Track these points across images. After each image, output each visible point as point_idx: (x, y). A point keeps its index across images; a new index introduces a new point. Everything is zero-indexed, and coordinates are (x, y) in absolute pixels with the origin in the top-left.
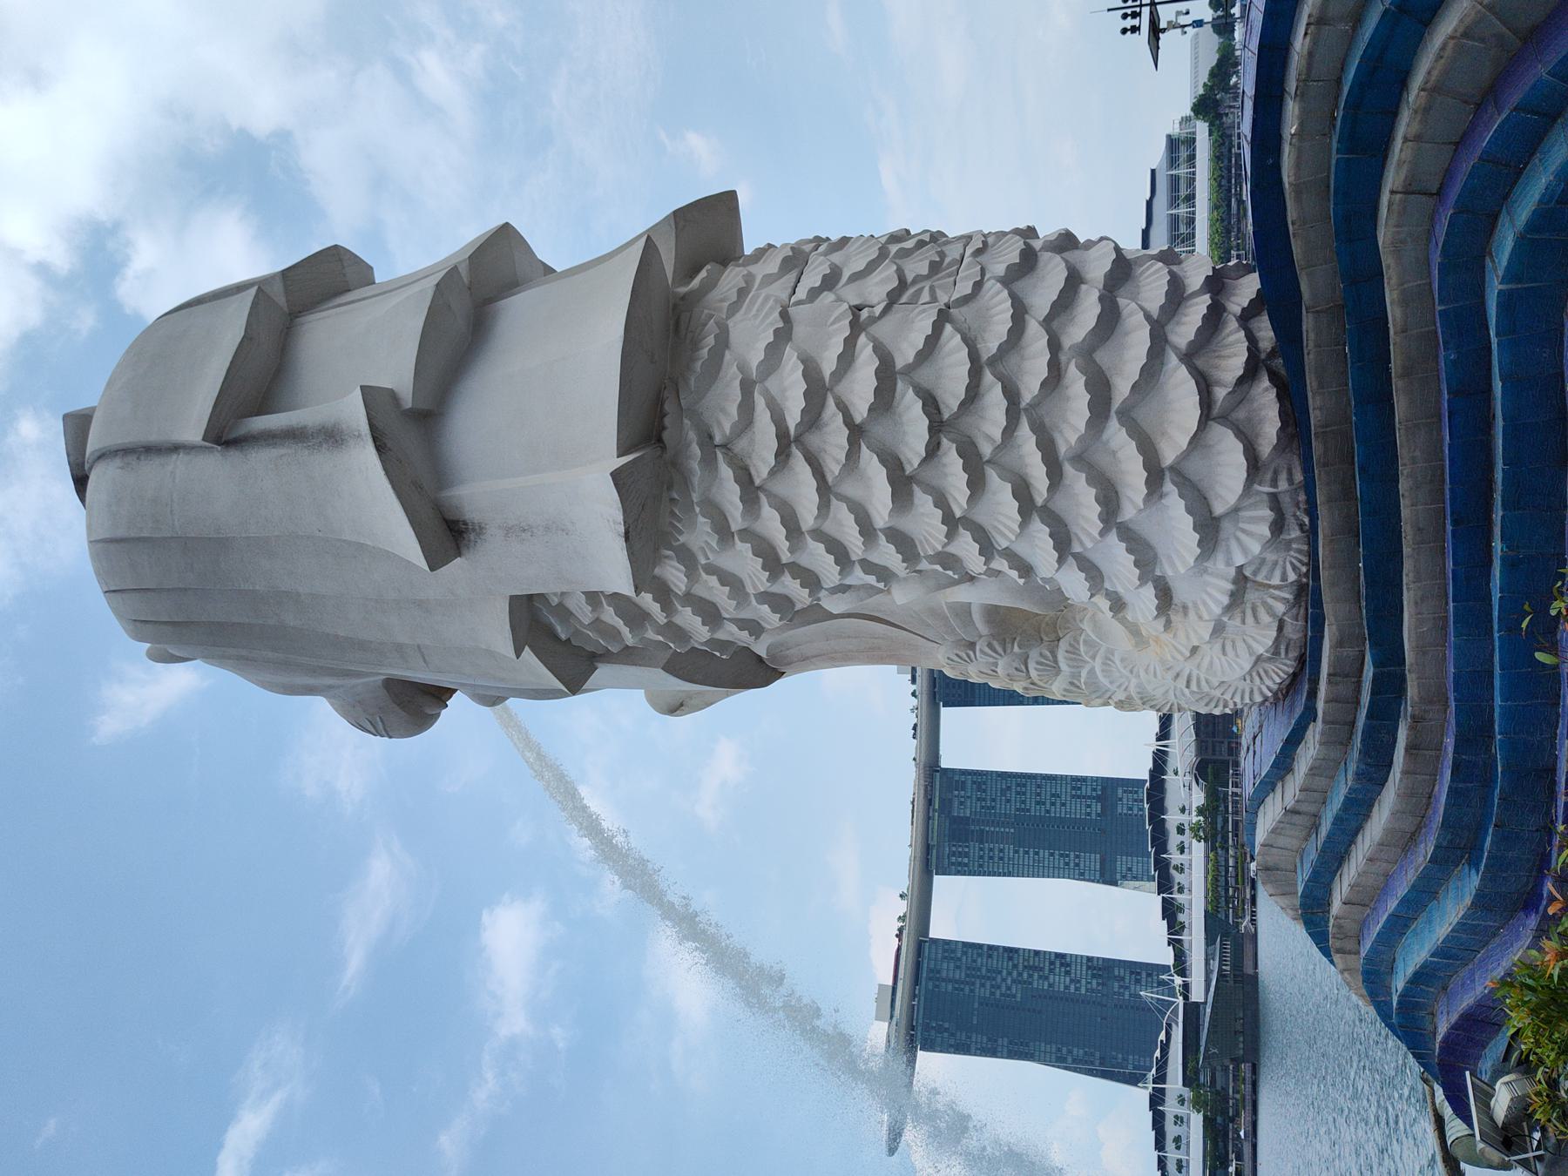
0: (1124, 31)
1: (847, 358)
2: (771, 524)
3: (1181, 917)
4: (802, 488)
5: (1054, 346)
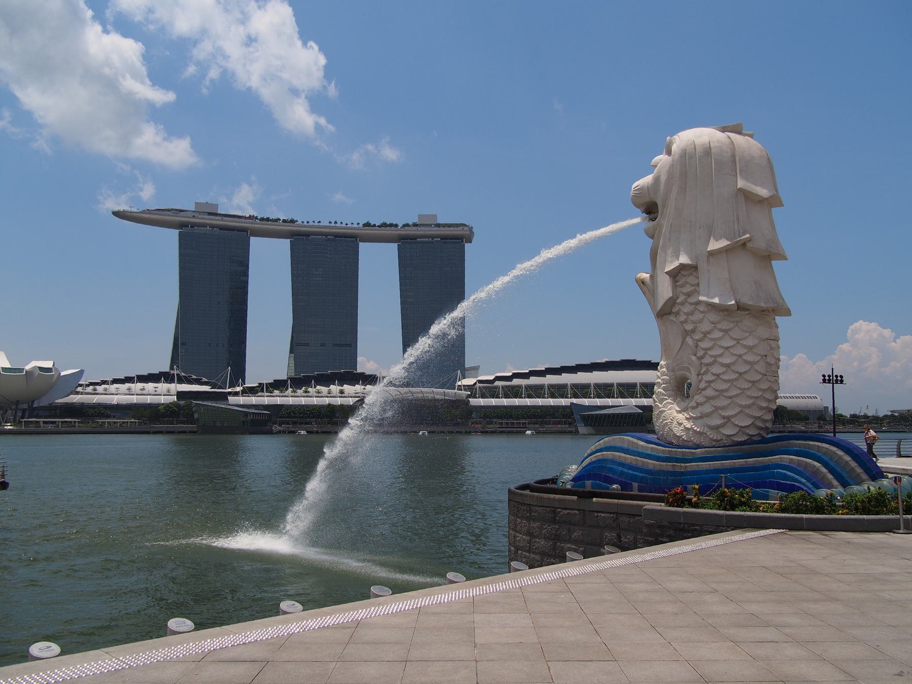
0: (824, 376)
1: (757, 354)
2: (717, 334)
3: (277, 392)
4: (728, 343)
5: (757, 398)
